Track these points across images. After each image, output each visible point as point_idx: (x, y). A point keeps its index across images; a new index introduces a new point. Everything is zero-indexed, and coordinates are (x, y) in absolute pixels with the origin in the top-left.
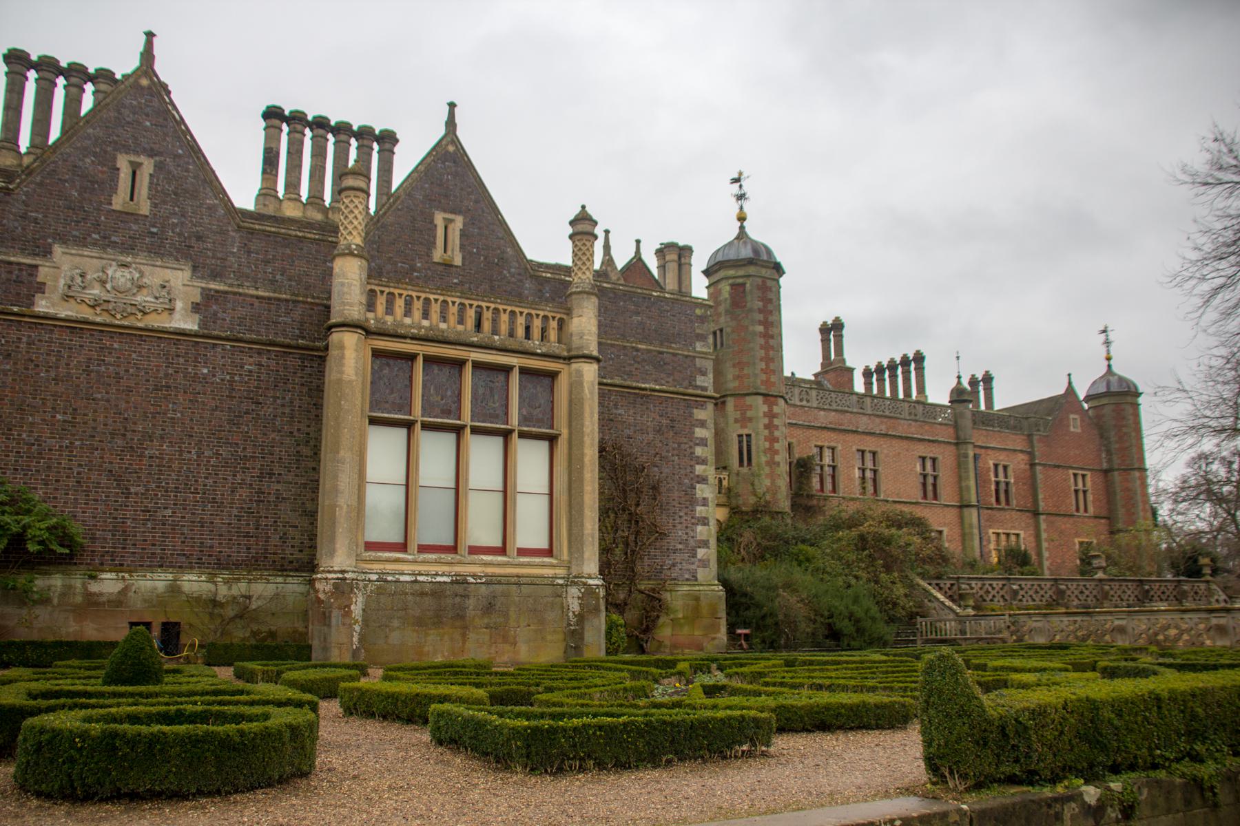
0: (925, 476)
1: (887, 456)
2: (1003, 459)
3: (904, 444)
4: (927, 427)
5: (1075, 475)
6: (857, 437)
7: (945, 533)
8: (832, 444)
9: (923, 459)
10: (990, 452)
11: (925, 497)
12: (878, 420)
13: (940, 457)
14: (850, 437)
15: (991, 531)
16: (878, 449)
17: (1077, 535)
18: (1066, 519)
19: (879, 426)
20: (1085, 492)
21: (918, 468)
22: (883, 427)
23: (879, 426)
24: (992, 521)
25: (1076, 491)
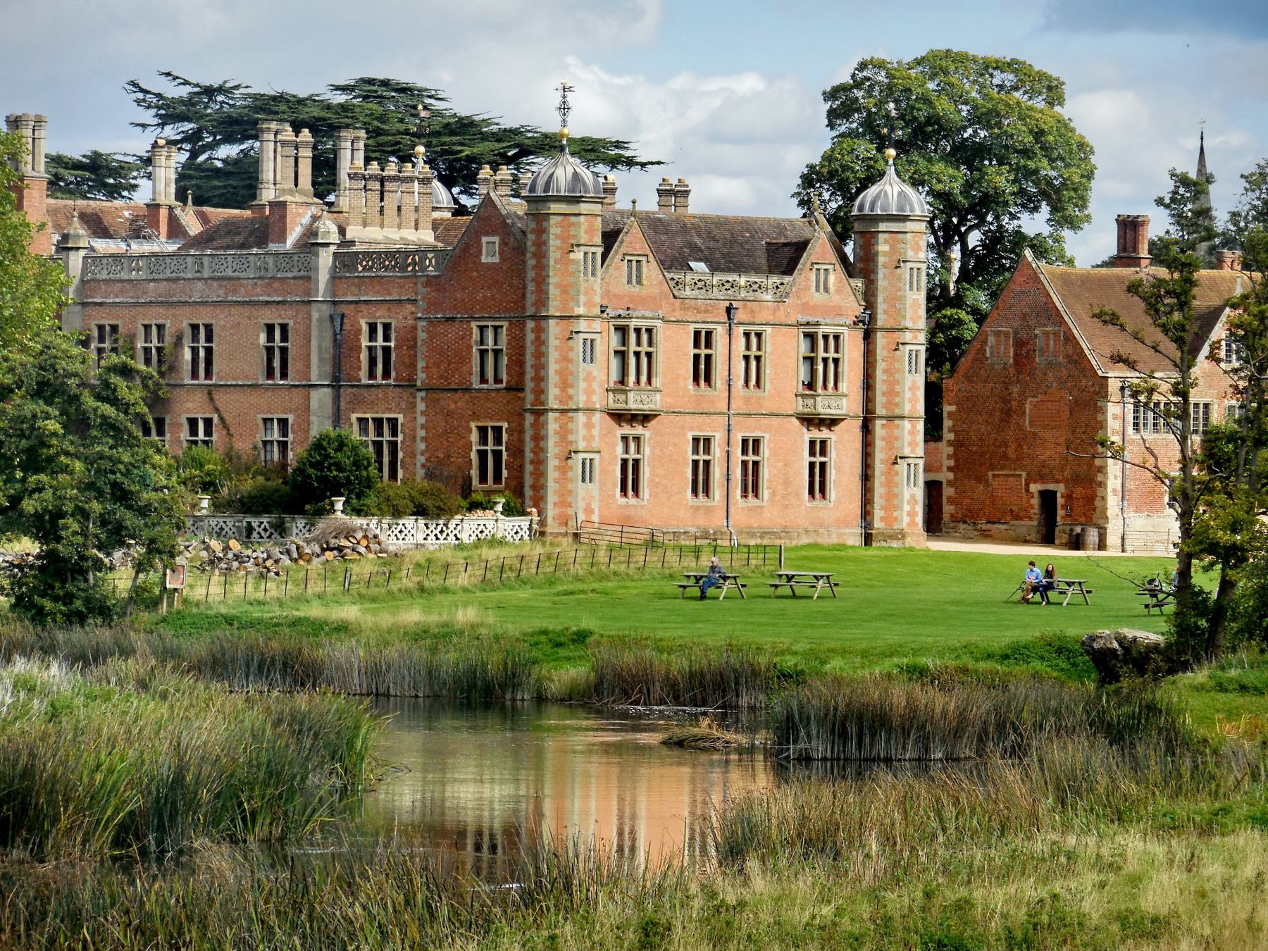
0: (270, 350)
1: (223, 328)
2: (381, 317)
3: (246, 311)
4: (276, 285)
5: (482, 328)
6: (188, 309)
7: (290, 422)
8: (160, 321)
9: (270, 329)
10: (363, 307)
11: (270, 374)
12: (215, 284)
13: (291, 323)
14: (179, 311)
15: (354, 417)
16: (213, 322)
17: (475, 416)
18: (460, 394)
19: (217, 293)
20: (497, 353)
21: (263, 338)
22: (221, 292)
23: (217, 293)
24: (356, 404)
25: (483, 353)
